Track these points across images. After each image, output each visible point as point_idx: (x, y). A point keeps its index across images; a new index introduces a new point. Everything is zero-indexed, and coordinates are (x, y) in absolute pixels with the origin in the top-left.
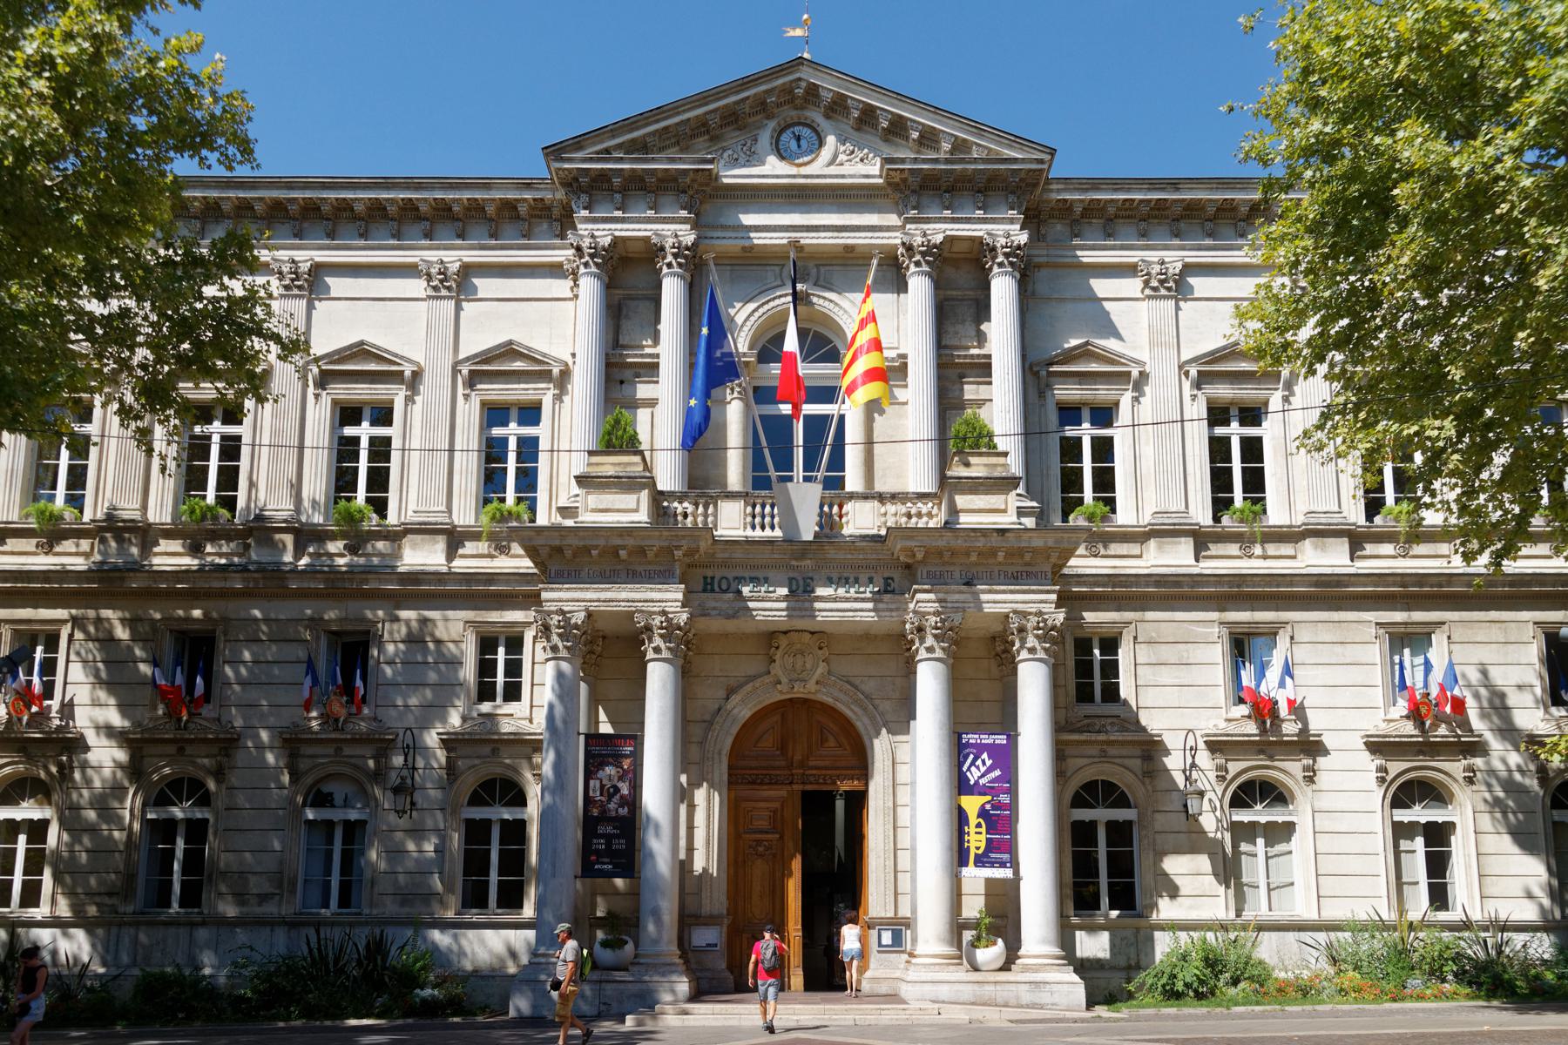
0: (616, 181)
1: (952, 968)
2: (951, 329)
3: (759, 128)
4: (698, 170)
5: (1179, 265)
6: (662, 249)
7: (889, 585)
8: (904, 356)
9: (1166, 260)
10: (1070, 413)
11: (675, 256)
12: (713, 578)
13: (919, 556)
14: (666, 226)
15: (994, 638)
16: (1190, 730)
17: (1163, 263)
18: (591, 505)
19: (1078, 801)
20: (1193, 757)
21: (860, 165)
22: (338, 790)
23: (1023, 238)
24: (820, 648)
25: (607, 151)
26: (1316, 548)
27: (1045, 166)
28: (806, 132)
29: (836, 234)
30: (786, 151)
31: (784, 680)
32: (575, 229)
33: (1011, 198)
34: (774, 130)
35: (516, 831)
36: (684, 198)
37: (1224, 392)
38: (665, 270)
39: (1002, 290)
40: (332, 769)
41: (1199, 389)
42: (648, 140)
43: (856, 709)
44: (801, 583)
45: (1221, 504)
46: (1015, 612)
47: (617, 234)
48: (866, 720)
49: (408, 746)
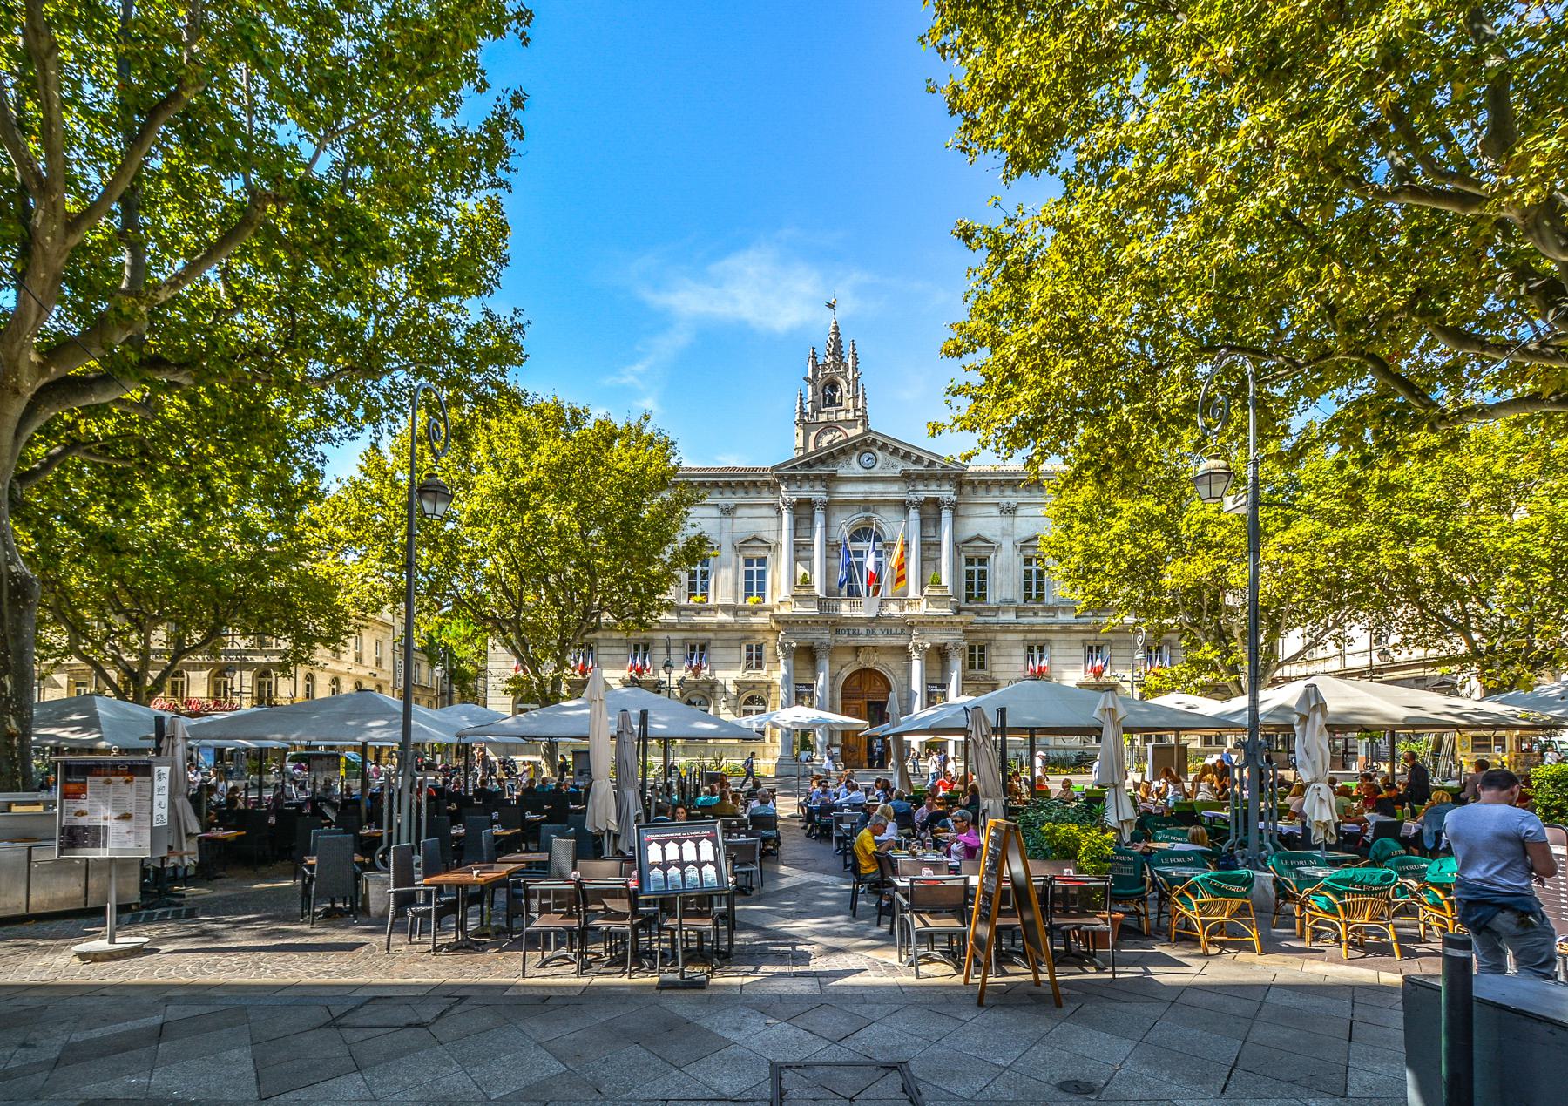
10: (970, 561)
39: (946, 516)
45: (1027, 597)
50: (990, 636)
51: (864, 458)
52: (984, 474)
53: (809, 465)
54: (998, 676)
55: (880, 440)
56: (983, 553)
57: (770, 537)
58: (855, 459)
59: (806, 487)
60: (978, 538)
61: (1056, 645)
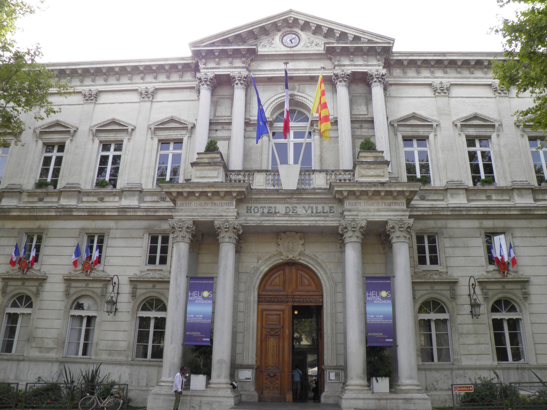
0: (217, 54)
1: (364, 392)
2: (356, 108)
3: (275, 35)
4: (249, 49)
5: (449, 84)
6: (234, 78)
7: (332, 210)
8: (337, 118)
9: (443, 82)
11: (239, 80)
12: (251, 207)
13: (345, 194)
14: (236, 70)
15: (380, 235)
16: (471, 277)
17: (442, 84)
18: (198, 176)
19: (421, 310)
20: (474, 288)
21: (316, 47)
22: (86, 302)
23: (384, 71)
24: (301, 239)
25: (213, 43)
26: (518, 196)
27: (391, 45)
28: (294, 36)
29: (306, 72)
30: (286, 43)
31: (284, 254)
32: (200, 72)
33: (378, 57)
34: (281, 35)
35: (161, 323)
36: (244, 59)
37: (472, 132)
38: (235, 86)
39: (377, 90)
40: (83, 293)
41: (462, 131)
42: (229, 39)
43: (318, 268)
44: (291, 209)
46: (390, 220)
47: (216, 73)
48: (322, 272)
49: (115, 283)
50: (440, 223)
51: (287, 39)
52: (412, 54)
53: (226, 41)
54: (455, 274)
55: (302, 20)
56: (422, 132)
57: (185, 116)
58: (277, 38)
59: (225, 64)
60: (414, 116)
61: (517, 233)
